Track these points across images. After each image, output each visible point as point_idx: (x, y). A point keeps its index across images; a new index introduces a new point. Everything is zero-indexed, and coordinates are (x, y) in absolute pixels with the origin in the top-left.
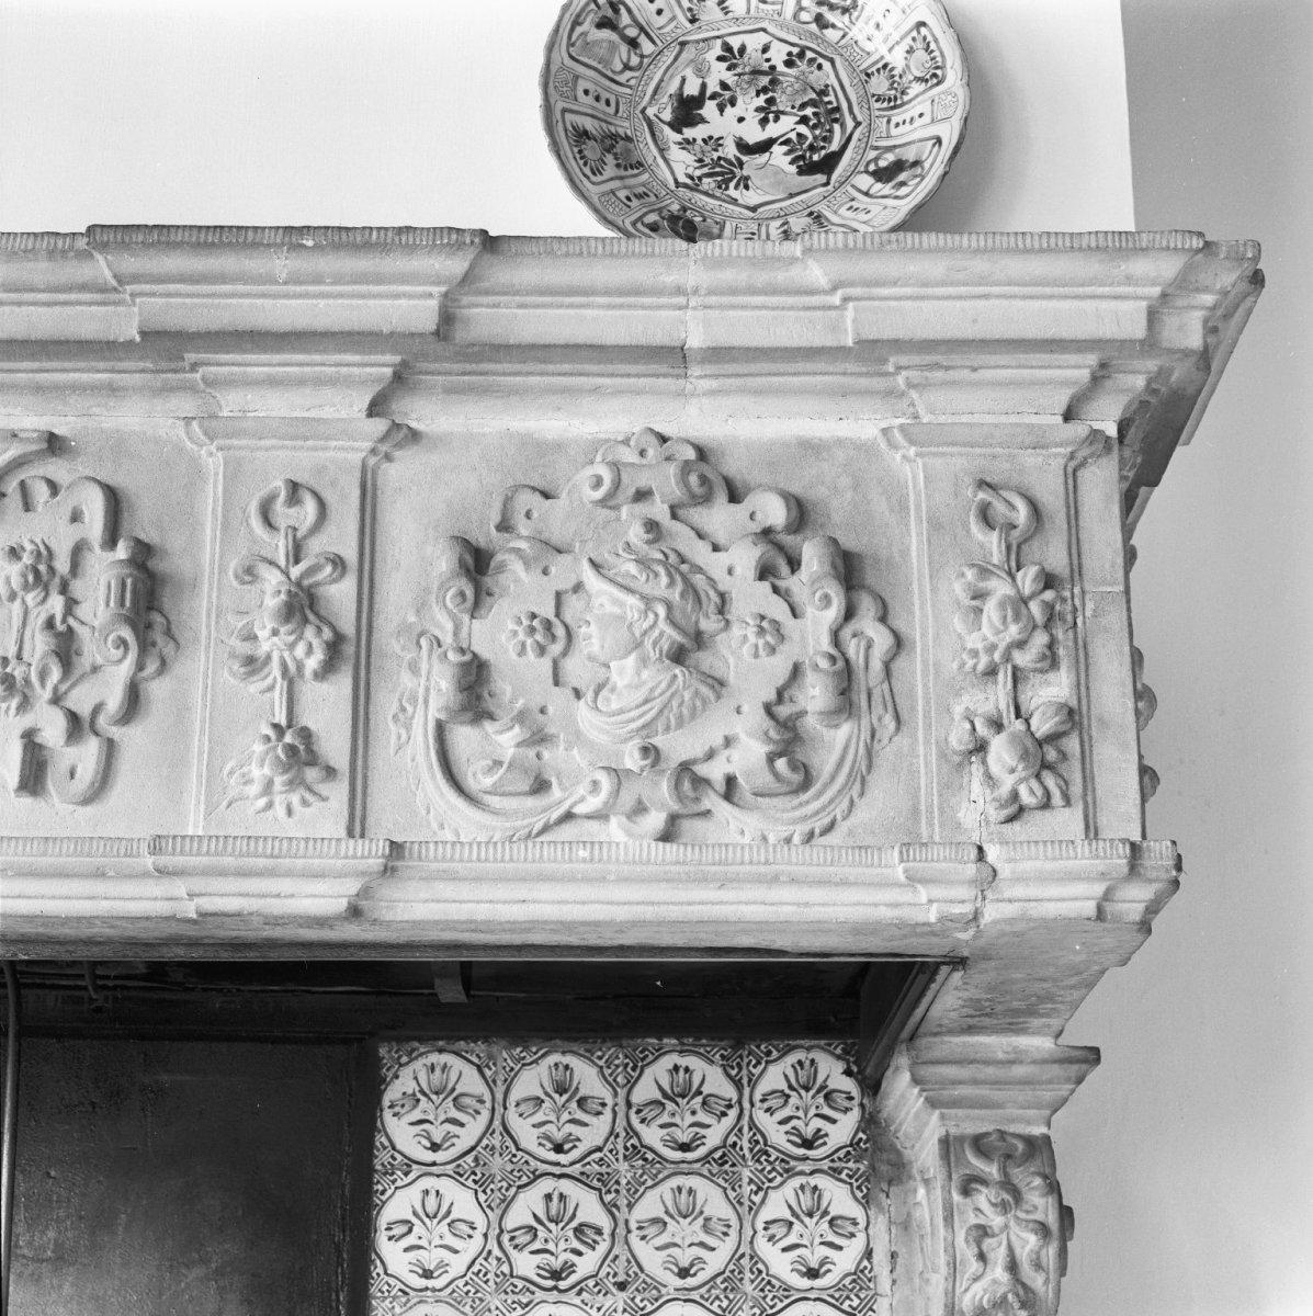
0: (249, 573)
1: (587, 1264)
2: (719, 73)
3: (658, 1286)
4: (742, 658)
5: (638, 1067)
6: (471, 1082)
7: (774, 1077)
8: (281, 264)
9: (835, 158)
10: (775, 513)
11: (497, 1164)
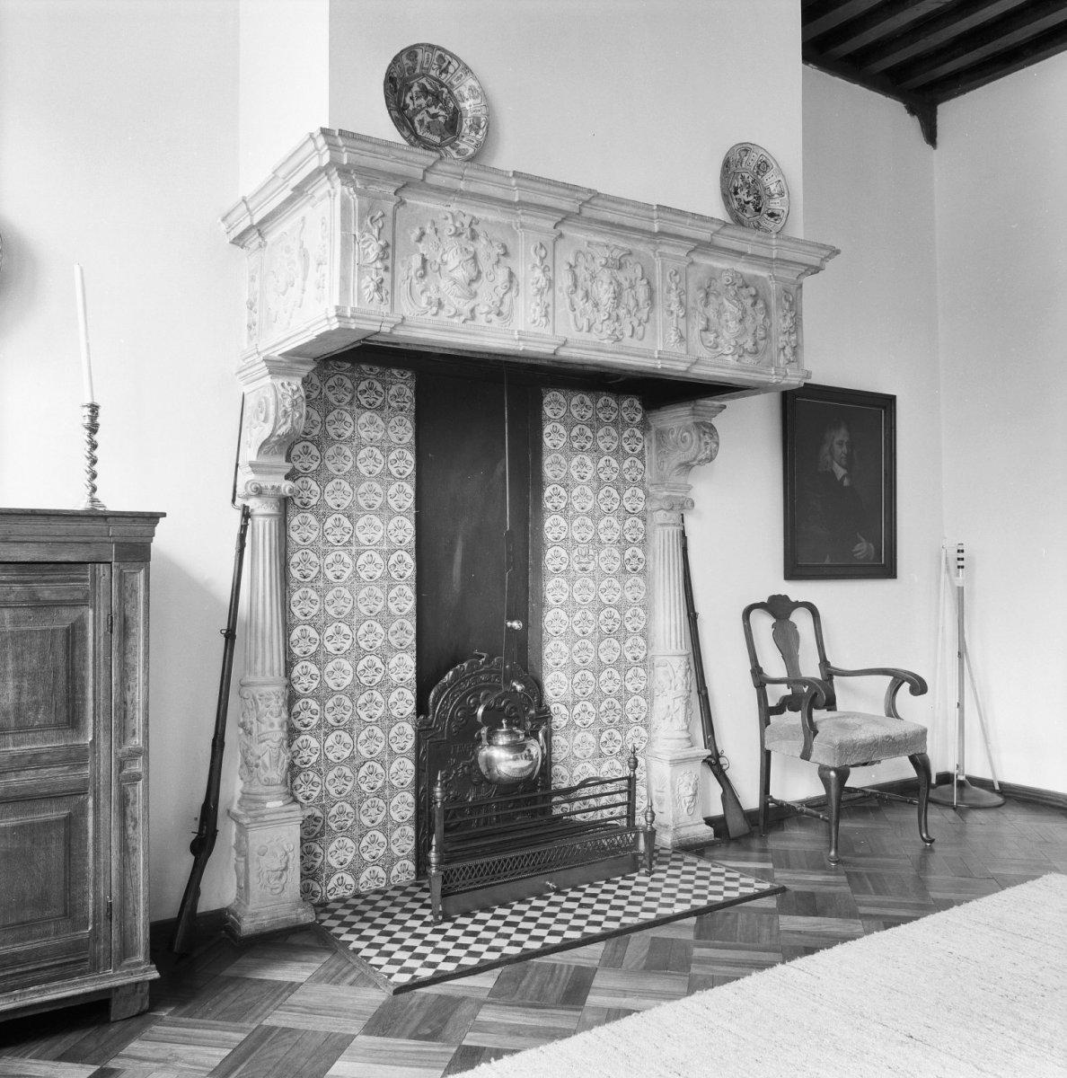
0: (669, 292)
1: (588, 446)
2: (741, 182)
3: (602, 451)
5: (598, 398)
6: (562, 399)
7: (625, 404)
8: (689, 221)
9: (761, 208)
11: (569, 420)
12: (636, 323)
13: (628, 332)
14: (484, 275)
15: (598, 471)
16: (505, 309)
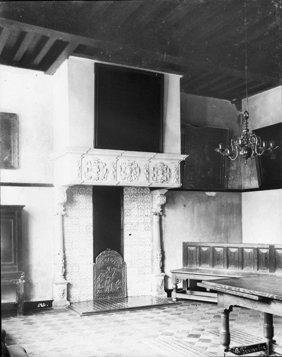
4: (165, 174)
10: (166, 167)
11: (130, 194)
12: (136, 177)
13: (134, 179)
14: (100, 170)
15: (138, 206)
16: (105, 177)
